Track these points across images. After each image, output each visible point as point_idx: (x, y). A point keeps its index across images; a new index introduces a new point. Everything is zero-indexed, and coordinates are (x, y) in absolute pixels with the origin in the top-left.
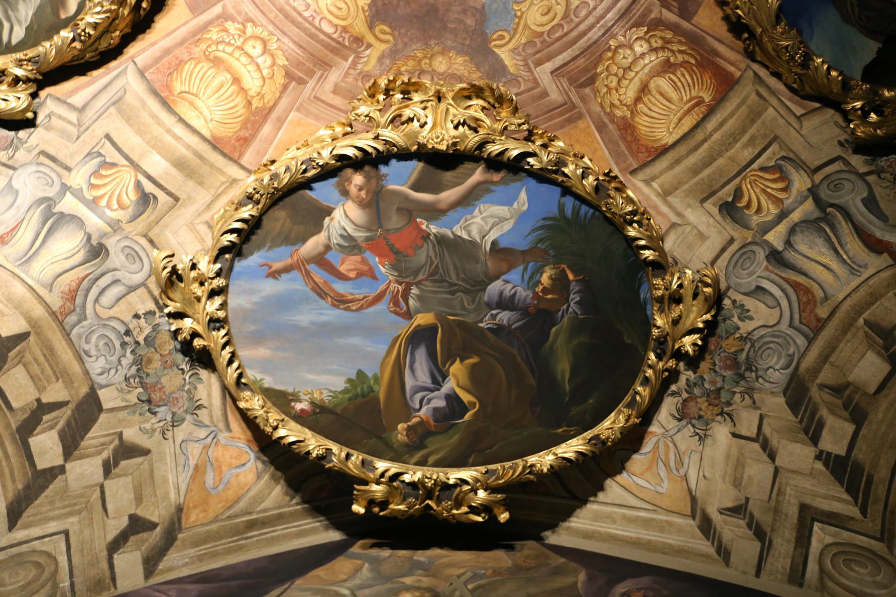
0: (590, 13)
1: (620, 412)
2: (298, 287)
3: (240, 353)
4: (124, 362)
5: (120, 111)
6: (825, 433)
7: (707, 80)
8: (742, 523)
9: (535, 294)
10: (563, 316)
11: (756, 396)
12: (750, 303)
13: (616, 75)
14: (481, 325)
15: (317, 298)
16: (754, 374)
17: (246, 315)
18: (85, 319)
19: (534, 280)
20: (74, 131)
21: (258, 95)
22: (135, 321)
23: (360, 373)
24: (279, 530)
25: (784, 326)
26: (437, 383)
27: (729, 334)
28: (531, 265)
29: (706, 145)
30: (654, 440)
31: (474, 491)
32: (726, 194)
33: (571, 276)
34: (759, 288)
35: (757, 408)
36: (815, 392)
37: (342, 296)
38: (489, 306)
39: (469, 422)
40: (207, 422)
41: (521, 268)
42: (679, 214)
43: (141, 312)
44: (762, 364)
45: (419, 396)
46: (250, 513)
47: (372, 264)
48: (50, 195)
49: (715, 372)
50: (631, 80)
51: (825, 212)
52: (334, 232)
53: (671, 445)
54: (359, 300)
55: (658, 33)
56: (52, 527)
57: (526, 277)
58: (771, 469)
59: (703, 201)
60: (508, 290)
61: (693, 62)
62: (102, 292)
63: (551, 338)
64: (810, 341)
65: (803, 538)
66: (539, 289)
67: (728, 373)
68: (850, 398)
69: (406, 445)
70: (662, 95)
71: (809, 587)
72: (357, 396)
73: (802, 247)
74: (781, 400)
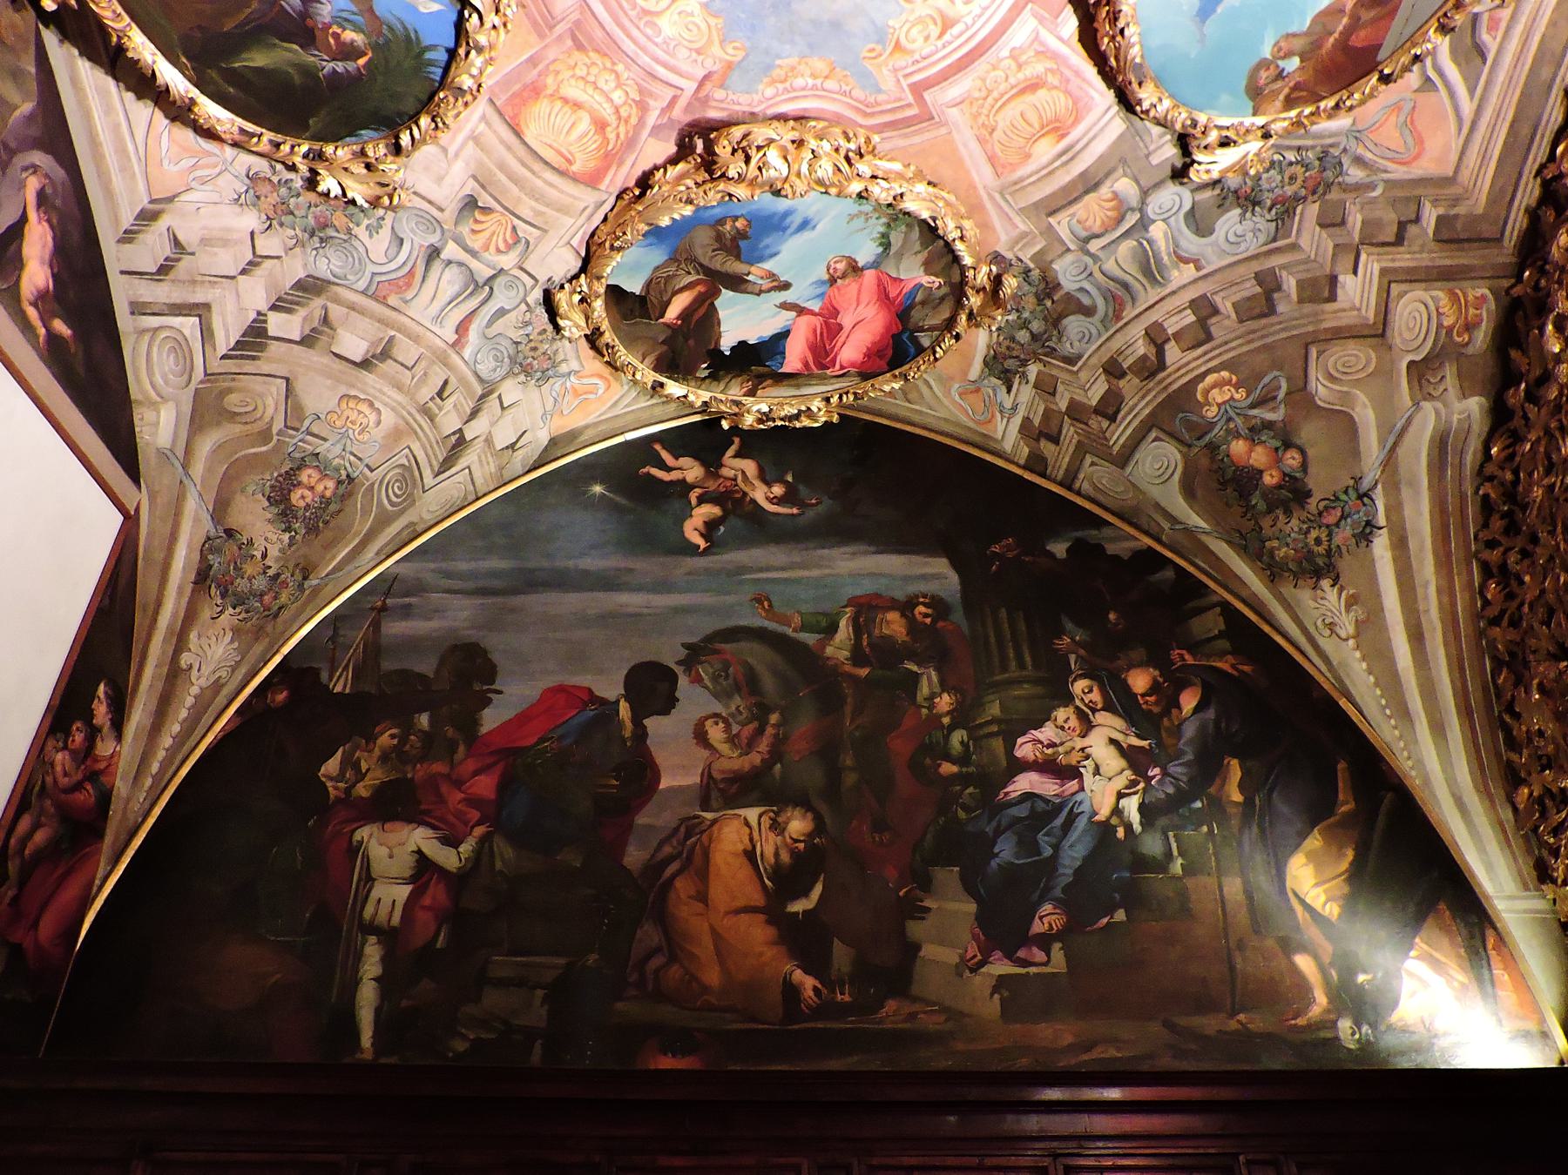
0: (648, 38)
6: (284, 315)
7: (592, 164)
9: (328, 26)
10: (315, 56)
11: (297, 250)
12: (385, 233)
13: (588, 74)
25: (371, 268)
29: (528, 174)
30: (218, 153)
32: (485, 200)
33: (362, 61)
34: (401, 241)
35: (286, 254)
36: (317, 304)
41: (355, 9)
42: (457, 155)
44: (330, 251)
49: (310, 207)
50: (585, 92)
51: (485, 284)
53: (217, 170)
55: (634, 110)
57: (344, 15)
59: (474, 177)
61: (610, 147)
63: (285, 45)
64: (363, 293)
66: (335, 29)
67: (311, 220)
68: (321, 333)
70: (574, 124)
71: (135, 321)
74: (302, 275)
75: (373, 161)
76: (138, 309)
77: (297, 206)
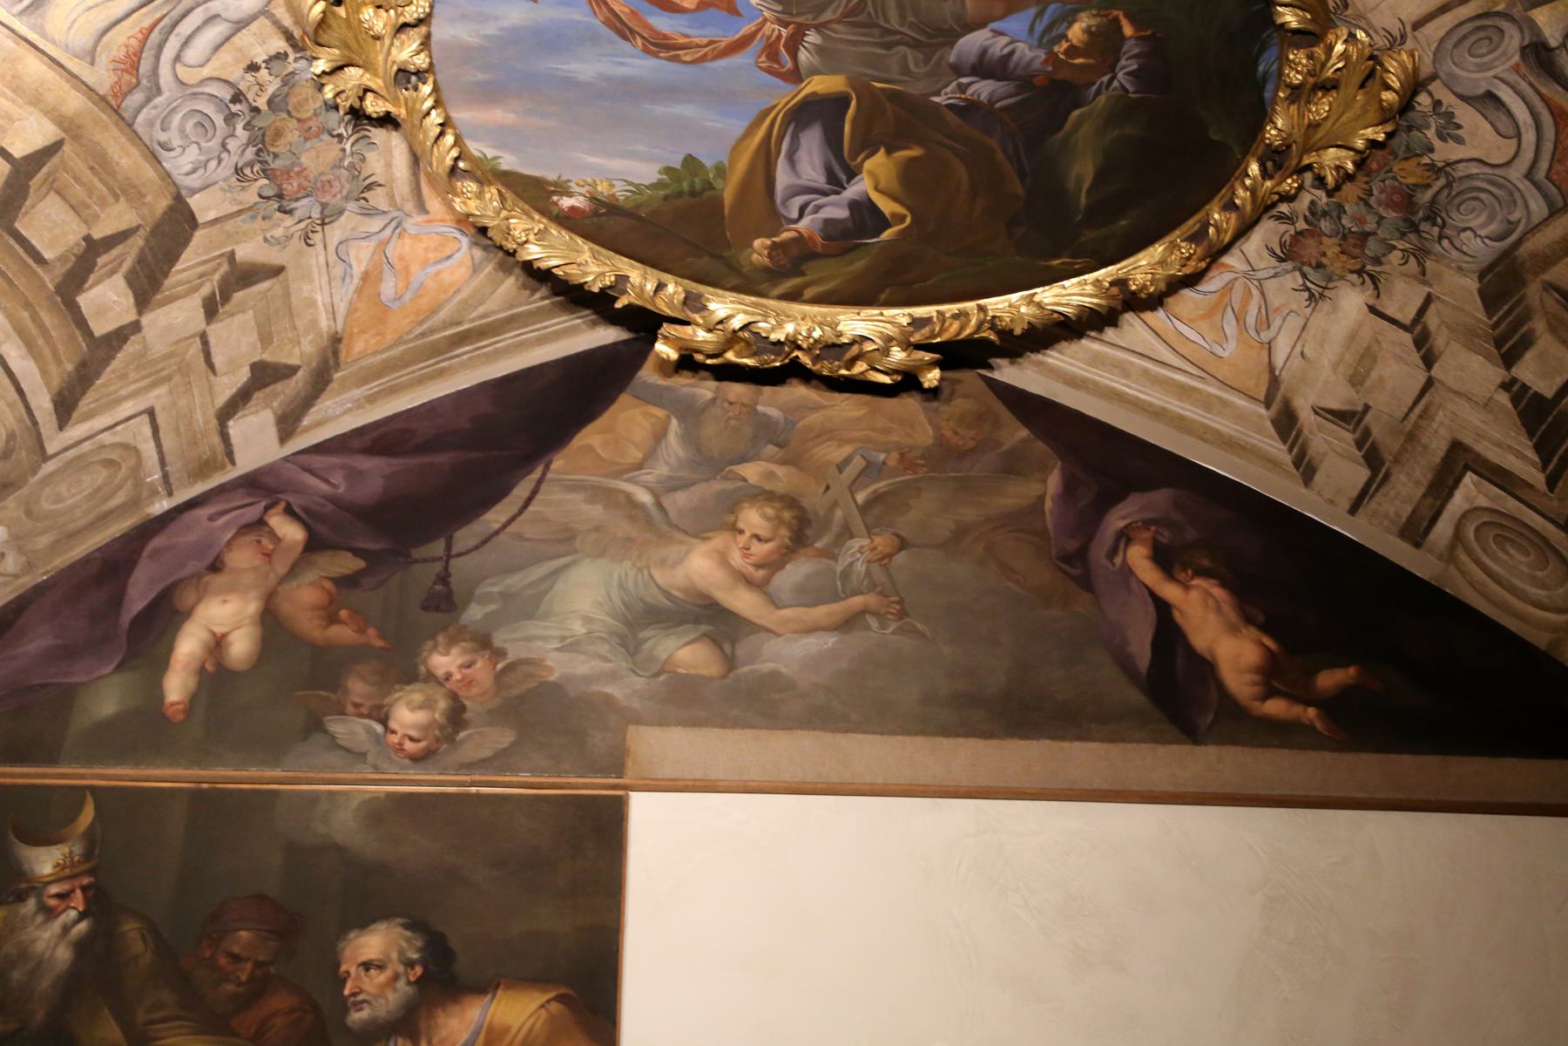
1: (1173, 246)
2: (578, 17)
3: (456, 115)
4: (232, 145)
6: (1529, 356)
8: (1349, 437)
9: (1051, 57)
10: (1098, 93)
11: (1428, 264)
14: (936, 99)
15: (616, 38)
16: (1436, 229)
17: (467, 55)
18: (159, 92)
19: (1054, 33)
22: (249, 77)
23: (690, 161)
24: (509, 338)
25: (1516, 174)
27: (1411, 154)
28: (1052, 8)
30: (1228, 277)
33: (1128, 30)
34: (1491, 97)
35: (1425, 283)
36: (1533, 292)
37: (665, 37)
38: (957, 70)
40: (384, 206)
41: (1032, 11)
43: (259, 60)
44: (1457, 219)
45: (799, 201)
46: (459, 323)
49: (1367, 204)
53: (1255, 292)
54: (699, 46)
56: (128, 408)
57: (1039, 27)
58: (1422, 378)
60: (999, 46)
62: (186, 42)
63: (1068, 125)
64: (1554, 212)
65: (1443, 484)
67: (1391, 215)
69: (766, 270)
72: (680, 194)
74: (1472, 284)
75: (1311, 80)
76: (1415, 530)
77: (1360, 221)
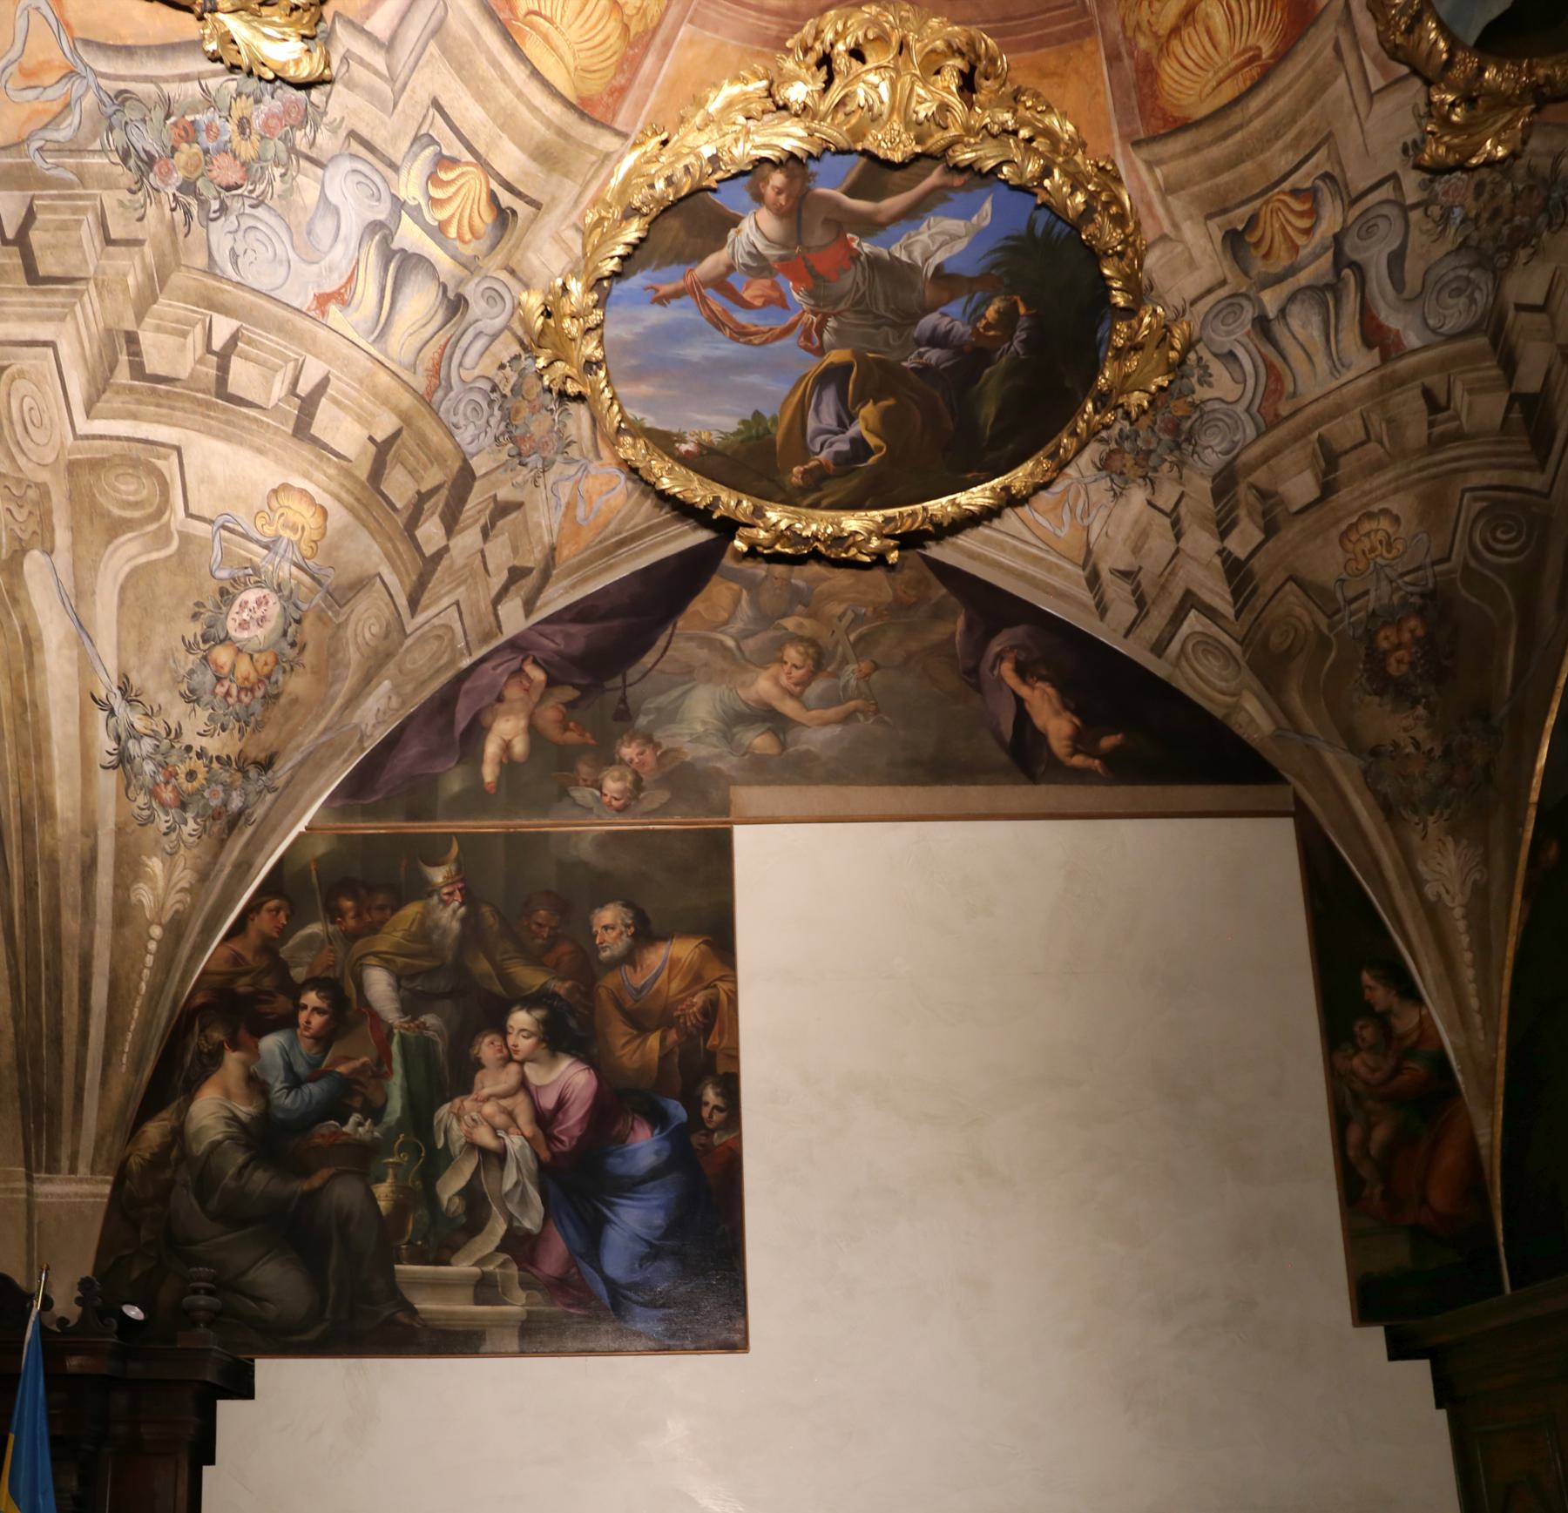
5: (445, 50)
20: (386, 89)
21: (638, 13)
23: (757, 414)
26: (843, 426)
31: (868, 541)
39: (872, 466)
47: (784, 290)
48: (381, 217)
52: (741, 249)
72: (750, 438)
73: (1295, 323)
